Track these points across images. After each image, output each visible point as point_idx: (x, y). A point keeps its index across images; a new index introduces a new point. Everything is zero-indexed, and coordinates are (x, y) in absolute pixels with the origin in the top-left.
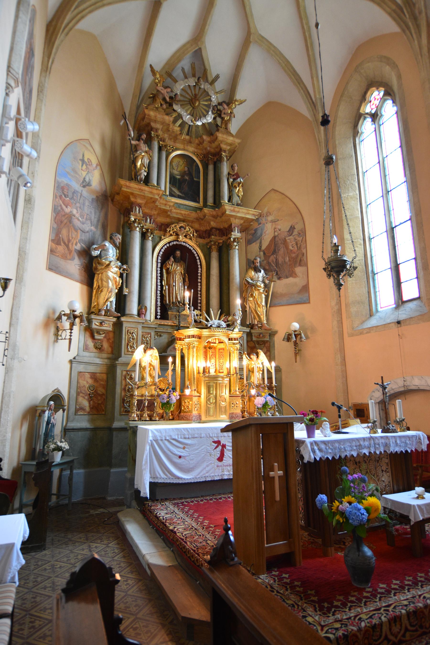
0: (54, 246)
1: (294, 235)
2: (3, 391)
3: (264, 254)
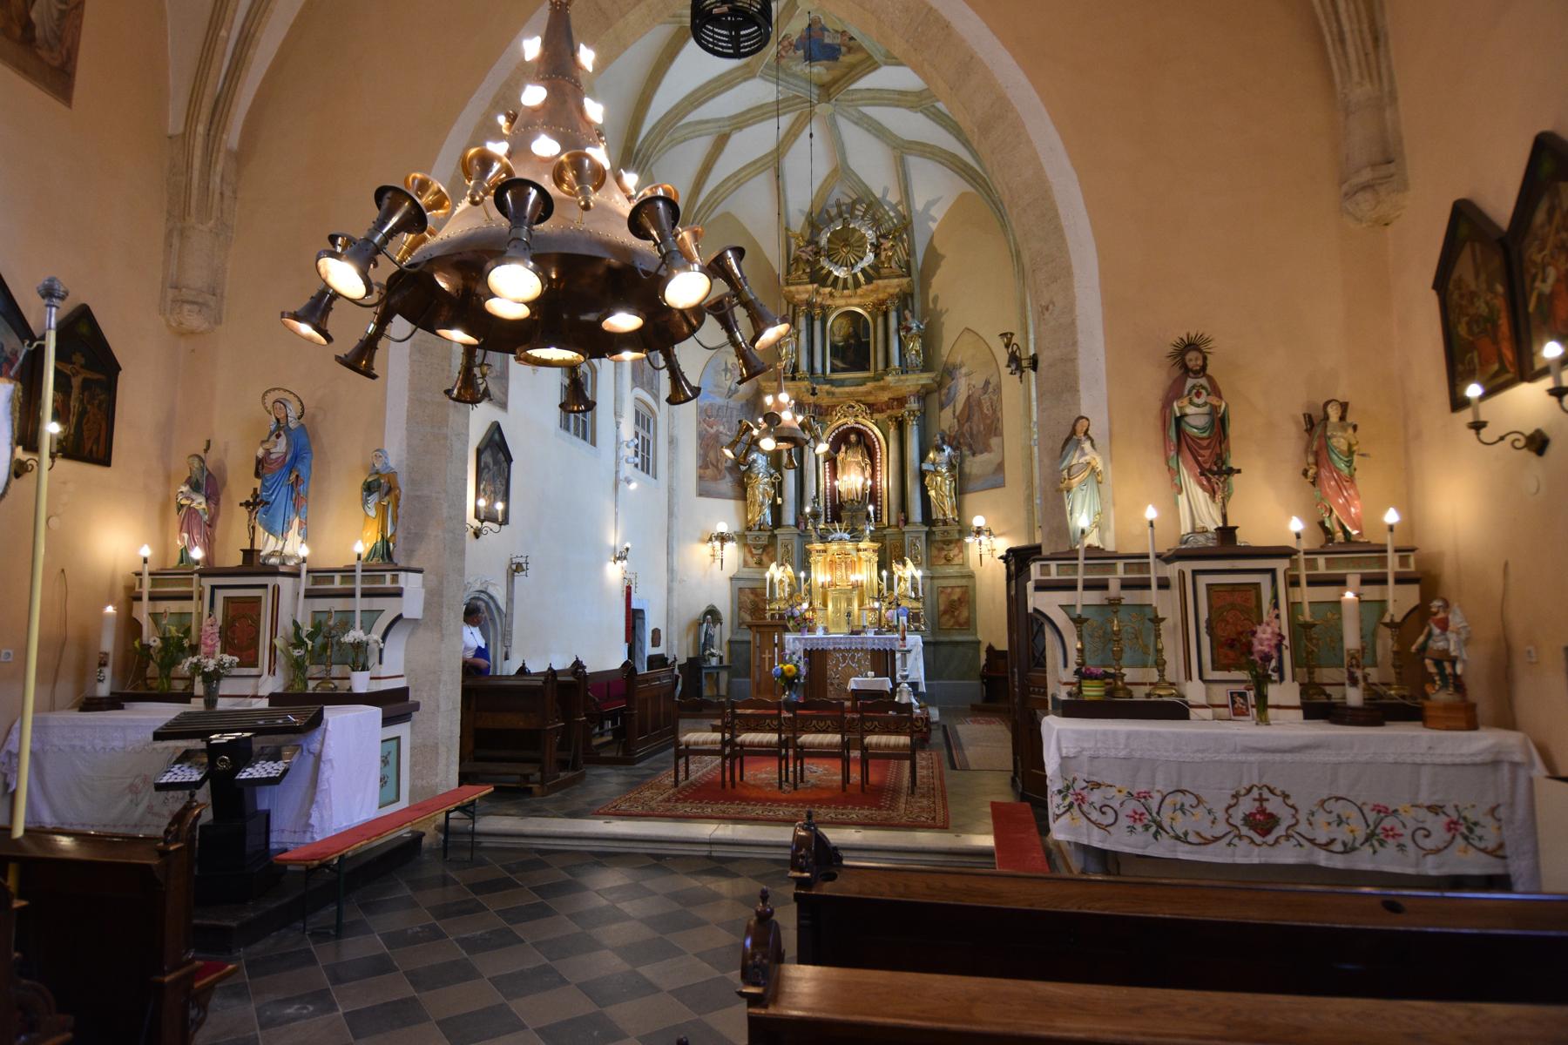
0: (702, 471)
3: (958, 421)
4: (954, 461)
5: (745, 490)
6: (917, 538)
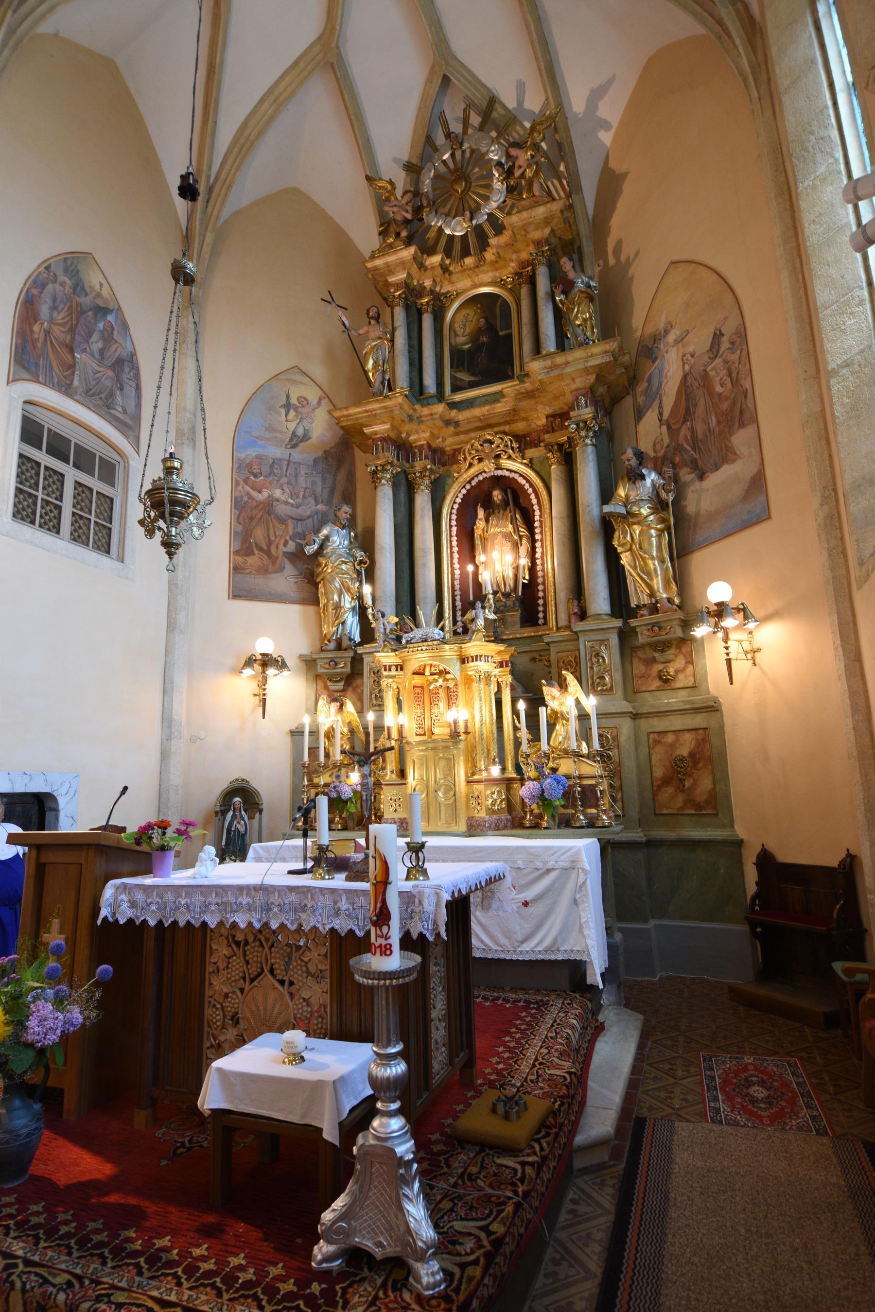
0: (240, 559)
1: (724, 352)
3: (669, 428)
4: (663, 495)
5: (316, 585)
6: (601, 642)
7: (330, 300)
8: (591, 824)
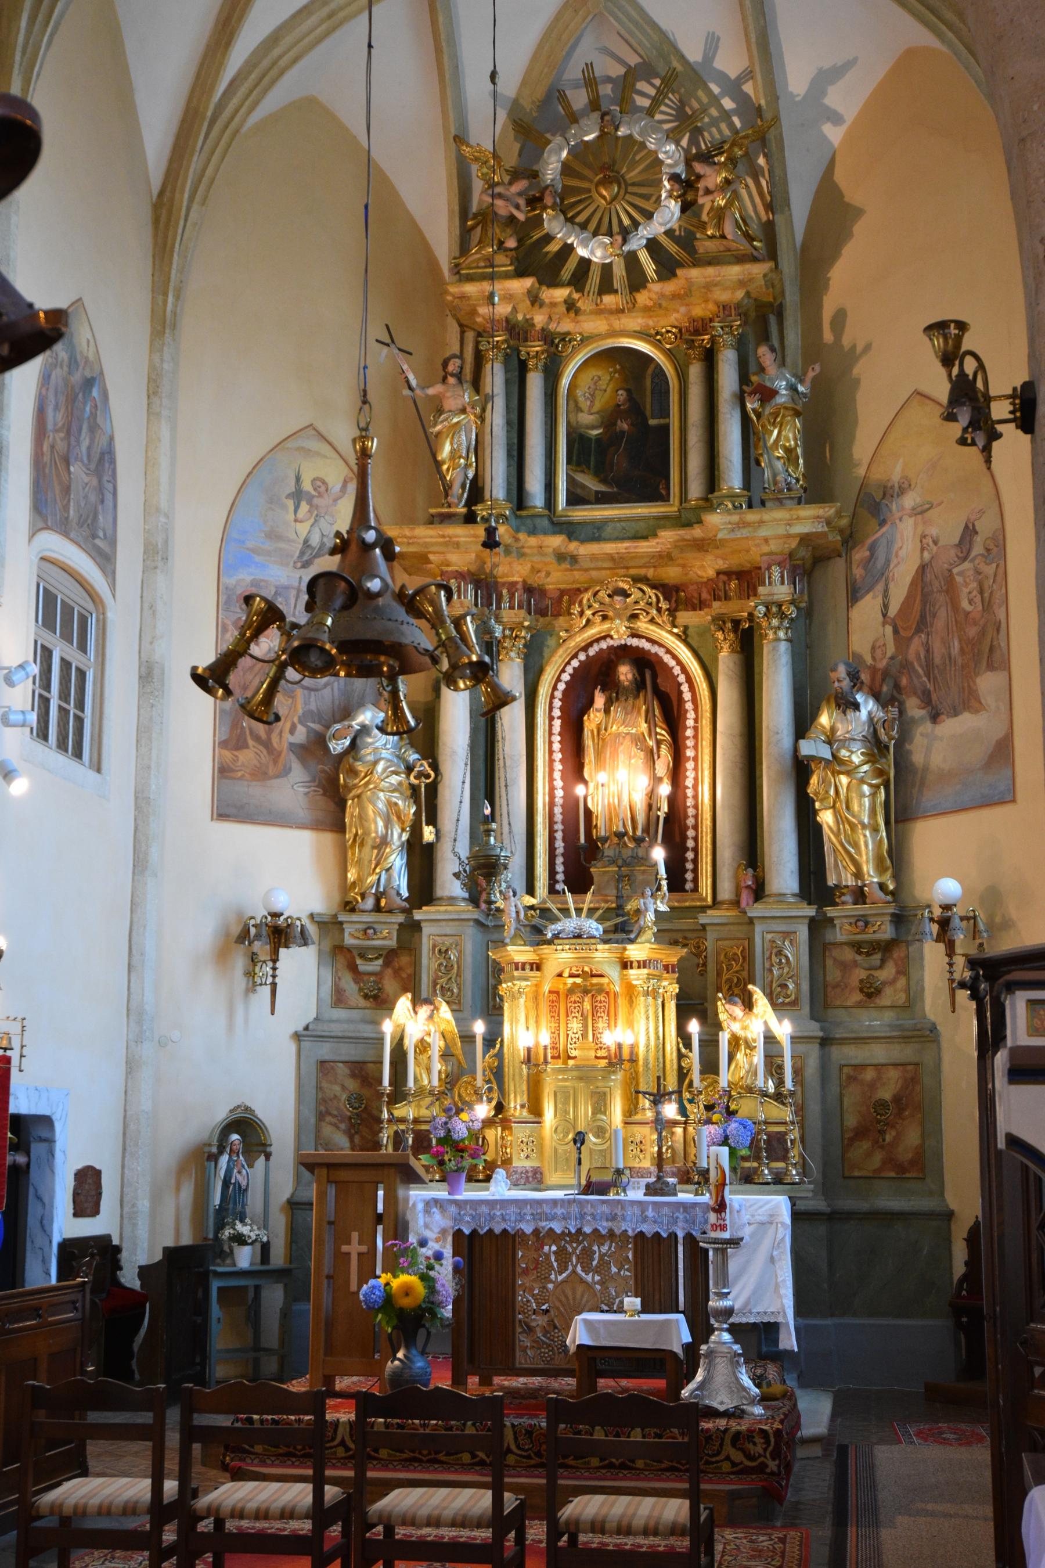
0: (227, 754)
1: (976, 556)
2: (125, 1111)
3: (896, 631)
5: (341, 805)
6: (786, 934)
7: (388, 341)
8: (779, 1180)
